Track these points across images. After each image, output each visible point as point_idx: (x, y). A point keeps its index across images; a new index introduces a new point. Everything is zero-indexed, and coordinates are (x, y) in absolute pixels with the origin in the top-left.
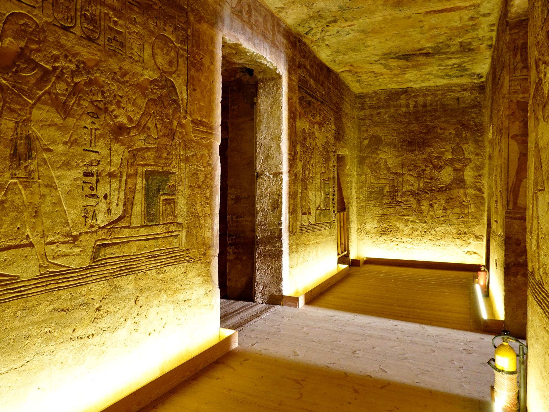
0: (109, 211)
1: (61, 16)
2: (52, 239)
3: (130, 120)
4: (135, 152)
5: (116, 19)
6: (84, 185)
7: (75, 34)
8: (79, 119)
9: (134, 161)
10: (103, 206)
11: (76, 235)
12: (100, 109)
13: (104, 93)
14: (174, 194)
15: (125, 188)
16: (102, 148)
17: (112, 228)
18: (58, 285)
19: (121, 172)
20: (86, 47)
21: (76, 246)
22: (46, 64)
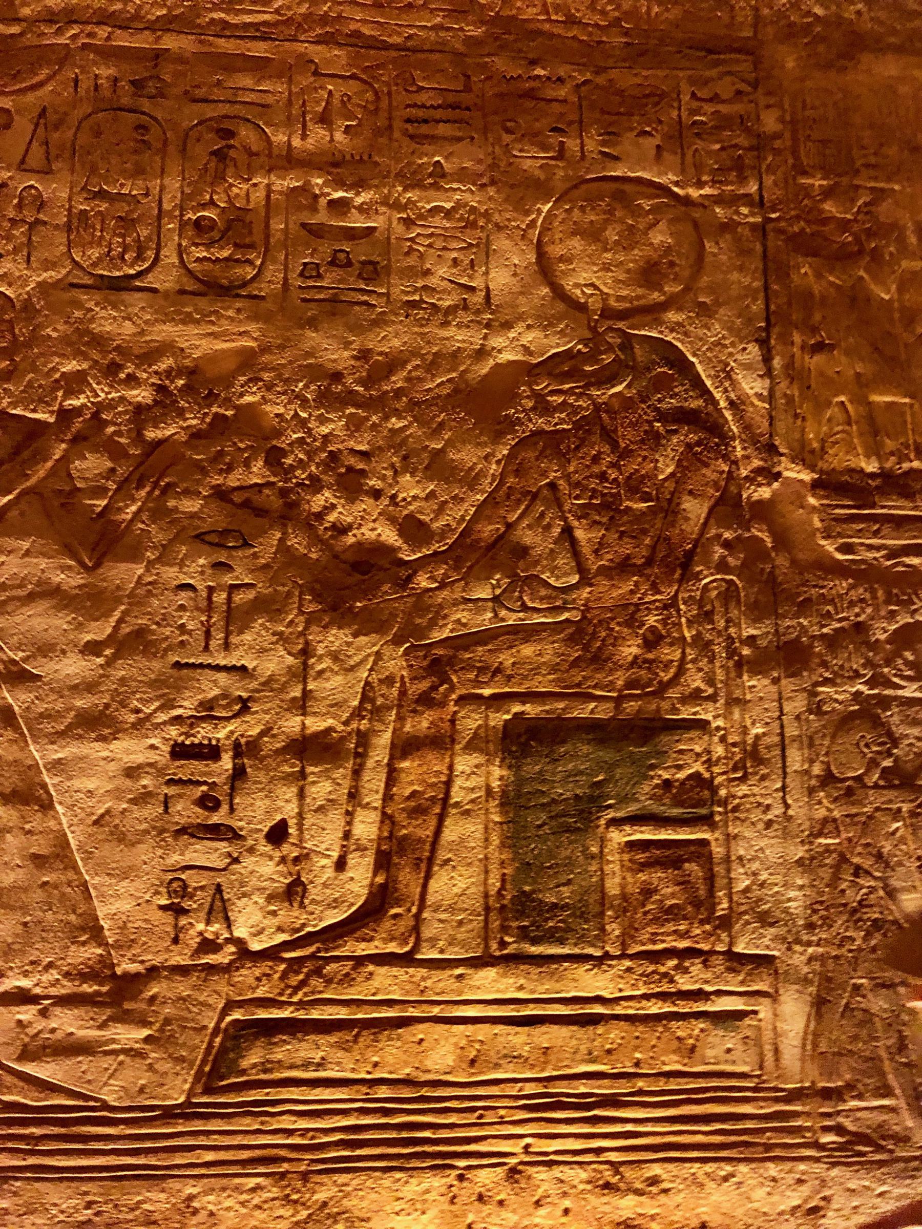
0: (294, 892)
1: (95, 253)
2: (25, 983)
3: (413, 529)
4: (440, 652)
5: (340, 194)
6: (171, 791)
7: (154, 291)
8: (159, 559)
9: (434, 688)
10: (265, 868)
11: (137, 975)
12: (261, 512)
13: (283, 453)
14: (707, 821)
15: (388, 797)
16: (263, 651)
17: (313, 956)
18: (32, 1161)
19: (364, 739)
20: (198, 322)
21: (125, 1018)
22: (34, 411)
